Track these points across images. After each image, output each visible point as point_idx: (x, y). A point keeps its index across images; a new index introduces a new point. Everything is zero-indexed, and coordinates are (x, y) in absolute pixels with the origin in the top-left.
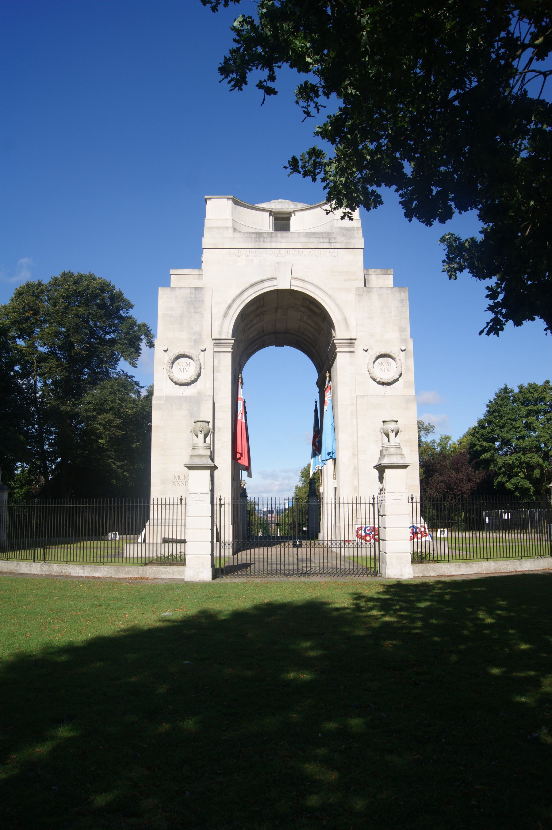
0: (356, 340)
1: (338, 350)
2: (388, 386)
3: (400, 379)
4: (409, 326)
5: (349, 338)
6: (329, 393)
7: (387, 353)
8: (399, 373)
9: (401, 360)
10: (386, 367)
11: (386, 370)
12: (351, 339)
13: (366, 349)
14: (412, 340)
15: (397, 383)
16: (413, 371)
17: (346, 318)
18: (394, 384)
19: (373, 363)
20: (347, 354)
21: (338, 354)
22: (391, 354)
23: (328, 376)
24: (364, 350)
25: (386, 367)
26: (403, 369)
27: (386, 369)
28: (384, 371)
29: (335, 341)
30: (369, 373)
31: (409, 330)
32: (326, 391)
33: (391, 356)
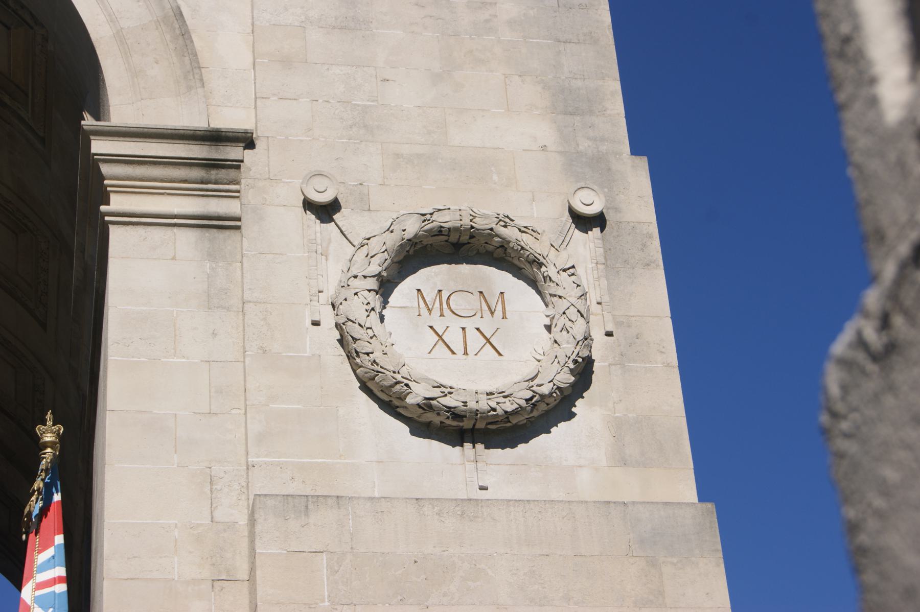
0: (249, 142)
1: (117, 203)
2: (497, 454)
3: (580, 407)
4: (617, 86)
5: (198, 122)
6: (50, 552)
7: (480, 224)
8: (569, 349)
9: (580, 270)
10: (477, 322)
11: (474, 341)
12: (215, 137)
13: (323, 198)
14: (642, 163)
15: (562, 429)
16: (673, 357)
17: (179, 15)
18: (541, 440)
19: (373, 284)
20: (186, 238)
21: (118, 237)
22: (510, 233)
23: (48, 438)
24: (309, 205)
25: (470, 325)
26: (598, 335)
27: (472, 334)
28: (458, 347)
29: (98, 146)
30: (352, 356)
31: (617, 107)
32: (34, 541)
33: (504, 245)
